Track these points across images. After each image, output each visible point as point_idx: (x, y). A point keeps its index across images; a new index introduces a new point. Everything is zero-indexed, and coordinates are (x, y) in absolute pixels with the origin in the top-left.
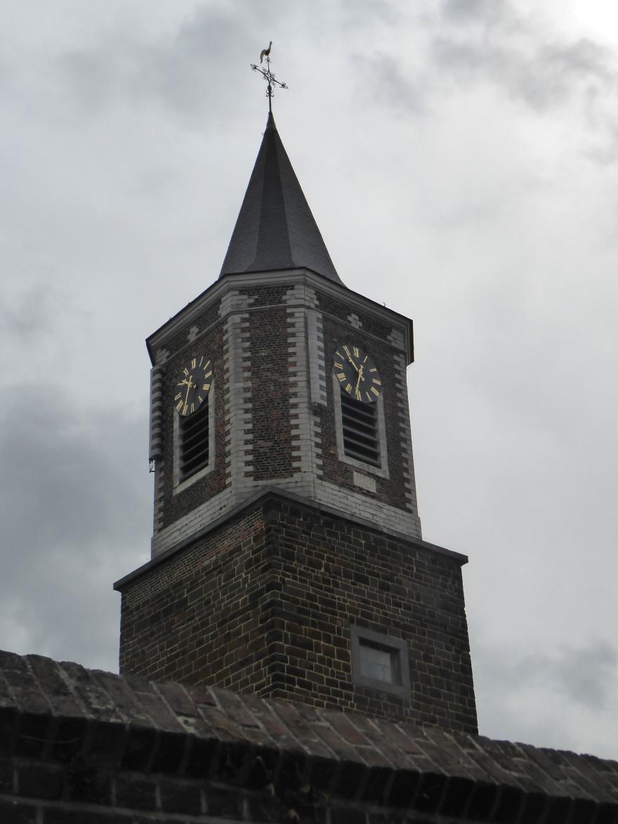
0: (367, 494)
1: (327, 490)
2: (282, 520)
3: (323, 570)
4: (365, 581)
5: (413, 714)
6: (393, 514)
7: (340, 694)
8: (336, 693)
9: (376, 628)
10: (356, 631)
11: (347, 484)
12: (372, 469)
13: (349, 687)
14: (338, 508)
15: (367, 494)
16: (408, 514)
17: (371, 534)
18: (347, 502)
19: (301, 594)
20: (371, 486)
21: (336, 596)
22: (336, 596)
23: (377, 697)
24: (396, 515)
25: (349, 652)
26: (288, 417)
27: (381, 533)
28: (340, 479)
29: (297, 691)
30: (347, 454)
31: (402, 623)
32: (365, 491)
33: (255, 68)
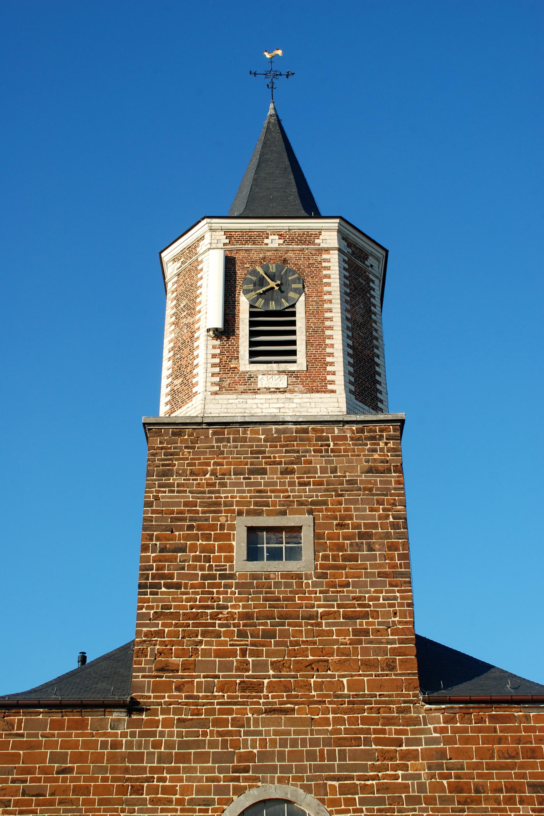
0: (278, 390)
1: (220, 402)
3: (208, 476)
4: (263, 472)
5: (315, 585)
6: (307, 400)
7: (219, 585)
8: (211, 586)
9: (270, 513)
11: (250, 390)
12: (283, 367)
13: (232, 576)
14: (233, 415)
15: (278, 390)
16: (332, 394)
17: (273, 427)
19: (178, 504)
20: (282, 382)
21: (223, 495)
22: (223, 495)
23: (267, 577)
24: (310, 400)
25: (234, 543)
26: (191, 351)
27: (284, 423)
28: (241, 388)
29: (163, 593)
30: (252, 363)
31: (310, 500)
32: (273, 390)
33: (255, 74)
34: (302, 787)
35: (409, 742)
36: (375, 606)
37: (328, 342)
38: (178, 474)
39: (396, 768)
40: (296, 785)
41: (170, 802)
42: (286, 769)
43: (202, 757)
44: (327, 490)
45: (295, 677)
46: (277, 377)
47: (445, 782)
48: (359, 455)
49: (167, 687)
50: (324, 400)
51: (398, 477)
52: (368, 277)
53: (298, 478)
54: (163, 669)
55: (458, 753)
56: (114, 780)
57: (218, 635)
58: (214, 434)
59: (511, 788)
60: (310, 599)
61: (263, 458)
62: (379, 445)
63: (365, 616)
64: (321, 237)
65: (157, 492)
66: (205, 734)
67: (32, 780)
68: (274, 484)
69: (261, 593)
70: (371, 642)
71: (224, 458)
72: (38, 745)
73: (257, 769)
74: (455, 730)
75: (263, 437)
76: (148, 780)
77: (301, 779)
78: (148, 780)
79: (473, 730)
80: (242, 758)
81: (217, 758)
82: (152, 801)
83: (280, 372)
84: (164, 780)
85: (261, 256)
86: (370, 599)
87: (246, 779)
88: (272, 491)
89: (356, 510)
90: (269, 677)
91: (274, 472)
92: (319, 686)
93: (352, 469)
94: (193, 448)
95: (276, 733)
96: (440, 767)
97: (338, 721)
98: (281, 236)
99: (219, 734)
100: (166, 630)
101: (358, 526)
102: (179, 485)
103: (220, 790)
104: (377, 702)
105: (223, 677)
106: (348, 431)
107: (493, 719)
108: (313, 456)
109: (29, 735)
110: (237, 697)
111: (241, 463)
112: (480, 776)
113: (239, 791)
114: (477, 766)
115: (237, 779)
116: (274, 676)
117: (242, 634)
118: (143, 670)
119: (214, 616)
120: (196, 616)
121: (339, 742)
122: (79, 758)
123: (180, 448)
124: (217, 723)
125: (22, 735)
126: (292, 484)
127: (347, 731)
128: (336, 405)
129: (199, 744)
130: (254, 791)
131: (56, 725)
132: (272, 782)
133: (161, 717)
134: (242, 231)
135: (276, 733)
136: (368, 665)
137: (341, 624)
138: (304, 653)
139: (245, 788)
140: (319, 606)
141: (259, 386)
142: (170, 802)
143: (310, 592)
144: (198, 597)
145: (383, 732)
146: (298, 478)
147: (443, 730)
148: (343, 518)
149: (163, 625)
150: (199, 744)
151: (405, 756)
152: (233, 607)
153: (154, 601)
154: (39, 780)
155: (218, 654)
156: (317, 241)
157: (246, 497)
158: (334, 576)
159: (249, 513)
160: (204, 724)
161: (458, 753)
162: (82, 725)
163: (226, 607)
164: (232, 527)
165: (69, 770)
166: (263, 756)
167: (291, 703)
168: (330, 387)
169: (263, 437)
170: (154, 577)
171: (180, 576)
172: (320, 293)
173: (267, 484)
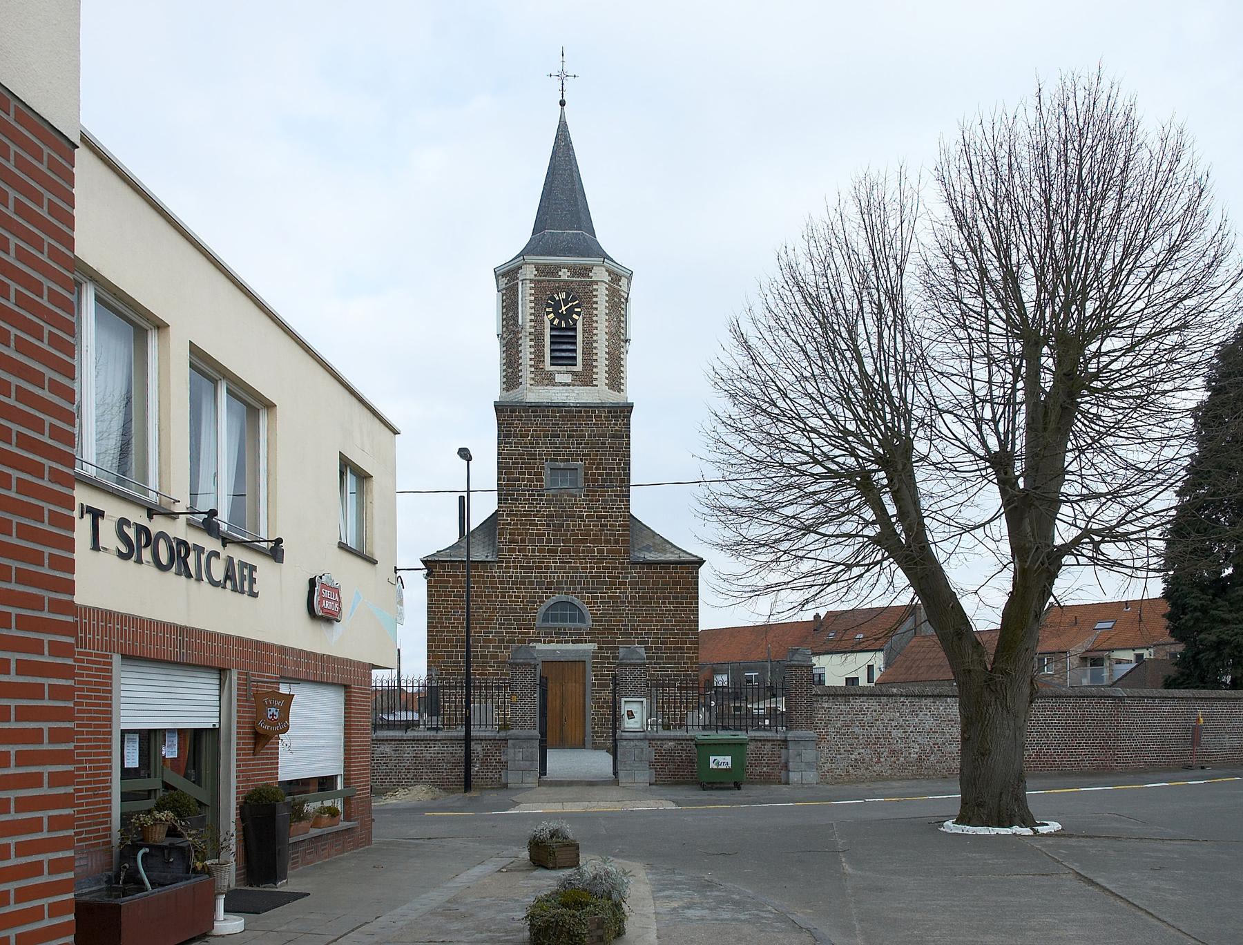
4: (558, 436)
5: (583, 500)
7: (536, 500)
12: (570, 368)
19: (515, 454)
30: (552, 365)
35: (623, 578)
37: (595, 351)
39: (616, 589)
49: (513, 550)
52: (620, 294)
55: (643, 583)
56: (493, 592)
59: (665, 598)
63: (606, 517)
66: (532, 573)
70: (609, 530)
74: (644, 573)
76: (507, 592)
78: (507, 592)
83: (568, 372)
86: (610, 508)
87: (550, 593)
89: (605, 460)
91: (564, 436)
92: (583, 551)
93: (604, 436)
97: (592, 568)
101: (605, 469)
111: (546, 431)
113: (547, 597)
114: (652, 588)
117: (548, 525)
119: (535, 516)
120: (525, 516)
124: (537, 568)
126: (573, 444)
137: (595, 521)
145: (612, 573)
147: (639, 573)
148: (598, 464)
150: (531, 577)
151: (620, 583)
153: (506, 507)
156: (590, 274)
159: (552, 460)
160: (531, 568)
161: (643, 583)
168: (595, 383)
170: (505, 495)
172: (591, 316)
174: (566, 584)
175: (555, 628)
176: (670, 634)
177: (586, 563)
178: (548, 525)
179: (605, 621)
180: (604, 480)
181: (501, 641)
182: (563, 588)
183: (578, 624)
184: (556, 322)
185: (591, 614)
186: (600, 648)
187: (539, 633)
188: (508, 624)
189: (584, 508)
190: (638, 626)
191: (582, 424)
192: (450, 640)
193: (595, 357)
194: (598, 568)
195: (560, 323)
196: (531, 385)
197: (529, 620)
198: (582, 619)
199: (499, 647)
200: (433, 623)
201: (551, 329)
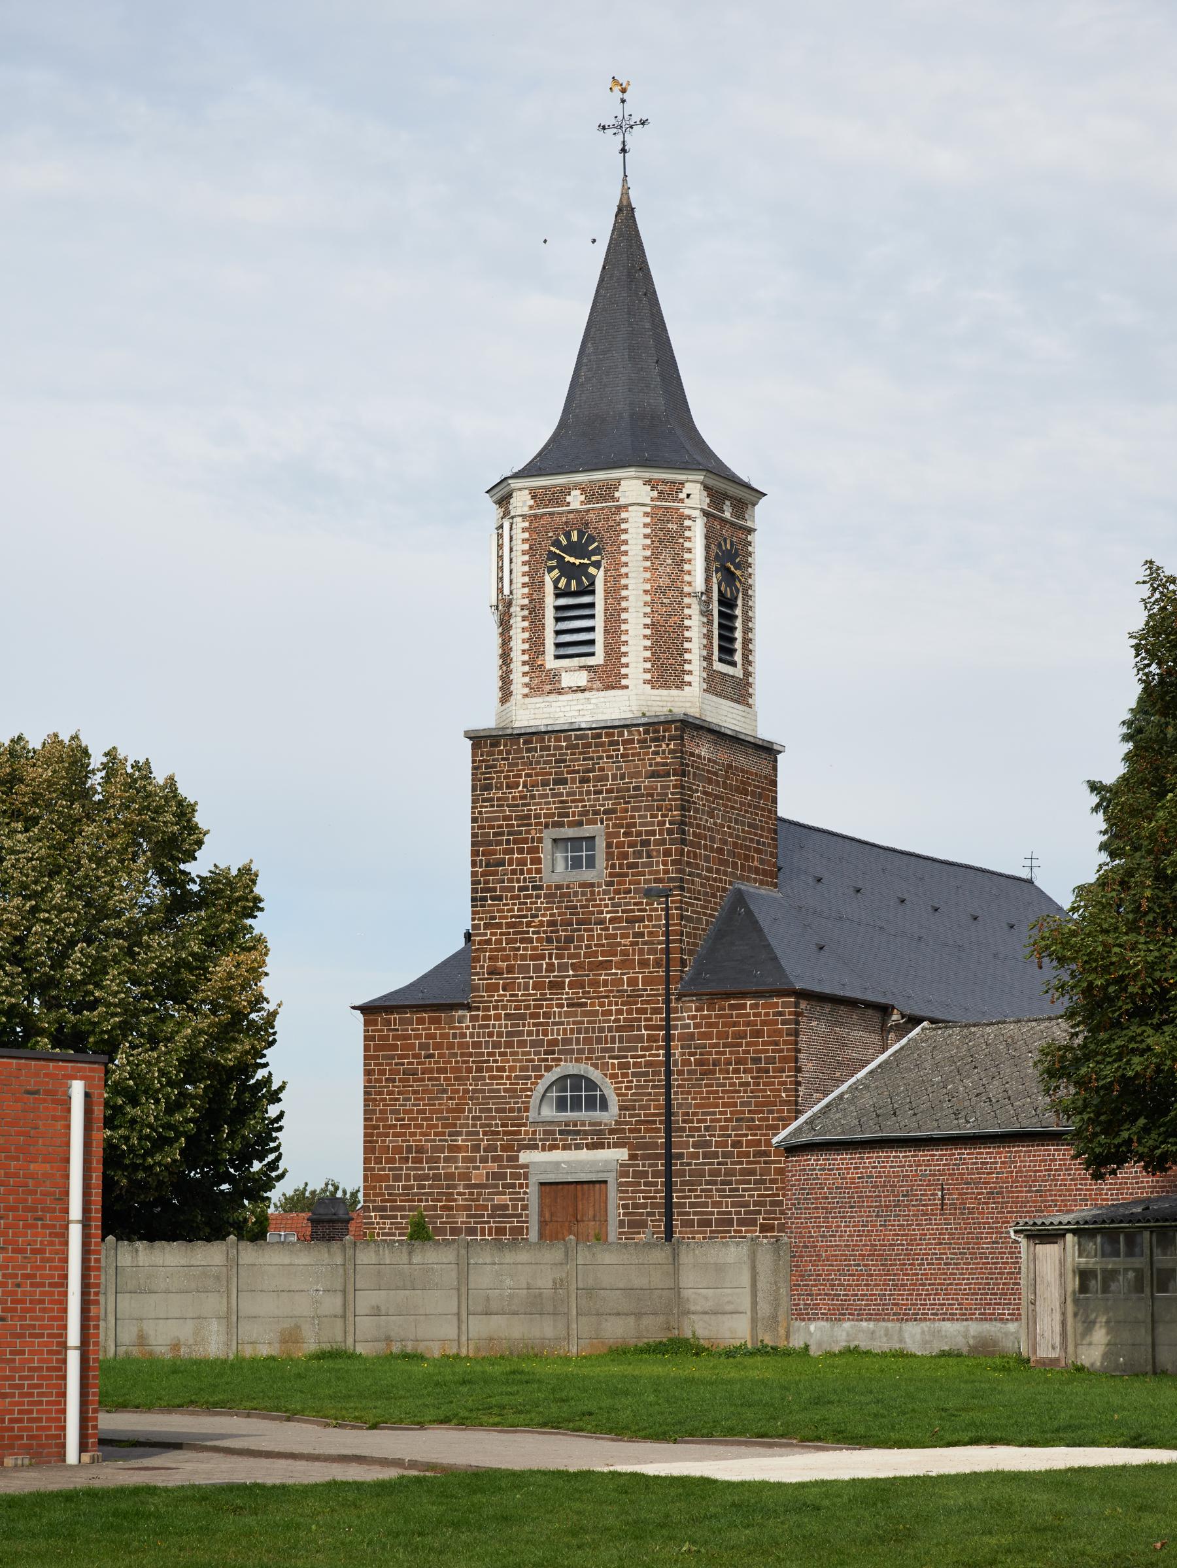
2: (482, 756)
3: (520, 788)
4: (564, 782)
5: (605, 892)
6: (602, 700)
7: (530, 896)
9: (572, 824)
10: (549, 834)
13: (540, 888)
16: (625, 691)
18: (552, 710)
19: (497, 819)
20: (582, 679)
23: (568, 887)
25: (542, 856)
28: (548, 688)
29: (490, 905)
30: (557, 657)
33: (604, 128)
34: (592, 1065)
36: (651, 910)
38: (497, 788)
40: (587, 1064)
41: (501, 1078)
42: (581, 1051)
43: (522, 1044)
44: (616, 798)
45: (588, 976)
46: (578, 673)
47: (692, 1058)
48: (644, 759)
50: (617, 699)
51: (676, 780)
53: (593, 786)
54: (493, 972)
57: (531, 941)
58: (524, 743)
59: (739, 1062)
60: (600, 906)
61: (565, 767)
62: (661, 746)
63: (641, 919)
64: (620, 488)
65: (482, 807)
66: (524, 1025)
67: (409, 1063)
68: (574, 794)
69: (563, 902)
71: (533, 769)
72: (409, 1037)
73: (561, 1052)
74: (703, 1017)
75: (564, 744)
77: (591, 1059)
79: (717, 1016)
80: (550, 1043)
81: (534, 1044)
82: (490, 1078)
84: (496, 1061)
85: (564, 519)
87: (553, 1060)
88: (573, 801)
90: (568, 976)
91: (573, 781)
92: (605, 983)
93: (637, 774)
94: (507, 759)
95: (574, 1023)
96: (689, 1047)
97: (619, 1012)
98: (583, 491)
99: (535, 1025)
100: (494, 938)
101: (639, 834)
102: (499, 799)
103: (537, 1069)
104: (648, 996)
105: (537, 977)
106: (636, 733)
107: (732, 1007)
108: (606, 763)
109: (403, 1030)
110: (546, 994)
112: (717, 1053)
113: (548, 1069)
114: (716, 1045)
115: (547, 1060)
116: (573, 976)
117: (549, 940)
118: (478, 974)
119: (529, 924)
121: (619, 1029)
122: (438, 1046)
123: (497, 760)
125: (397, 1030)
126: (588, 792)
127: (625, 1020)
128: (627, 703)
129: (520, 1033)
130: (558, 1069)
131: (421, 1021)
132: (571, 1061)
133: (492, 1013)
134: (546, 488)
135: (574, 1023)
136: (644, 964)
138: (595, 954)
139: (552, 1066)
140: (608, 912)
141: (563, 685)
142: (501, 1078)
143: (601, 900)
144: (516, 908)
146: (593, 786)
147: (694, 1017)
149: (492, 934)
150: (520, 1033)
152: (543, 915)
154: (412, 1063)
155: (533, 958)
157: (551, 809)
158: (619, 883)
160: (522, 1017)
162: (437, 1021)
163: (537, 916)
164: (540, 840)
165: (432, 1056)
166: (566, 1041)
167: (586, 998)
168: (624, 682)
169: (564, 744)
171: (503, 889)
172: (618, 565)
173: (568, 794)
174: (578, 1043)
175: (559, 1123)
176: (749, 1128)
177: (610, 1004)
178: (549, 940)
179: (641, 1107)
180: (638, 855)
181: (476, 1148)
182: (572, 1052)
183: (597, 1115)
184: (562, 583)
185: (618, 1095)
186: (632, 1157)
187: (534, 1133)
188: (487, 1118)
189: (606, 906)
190: (695, 1114)
191: (601, 758)
192: (397, 1150)
193: (624, 638)
194: (630, 1012)
195: (568, 584)
196: (526, 696)
197: (519, 1110)
198: (604, 1106)
199: (472, 1160)
200: (371, 1119)
201: (558, 596)
